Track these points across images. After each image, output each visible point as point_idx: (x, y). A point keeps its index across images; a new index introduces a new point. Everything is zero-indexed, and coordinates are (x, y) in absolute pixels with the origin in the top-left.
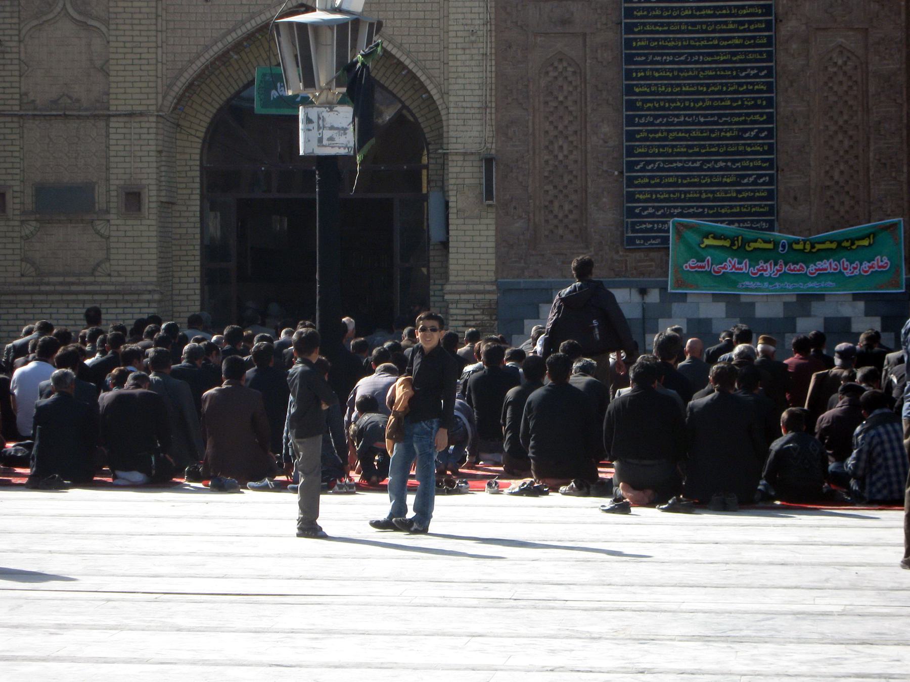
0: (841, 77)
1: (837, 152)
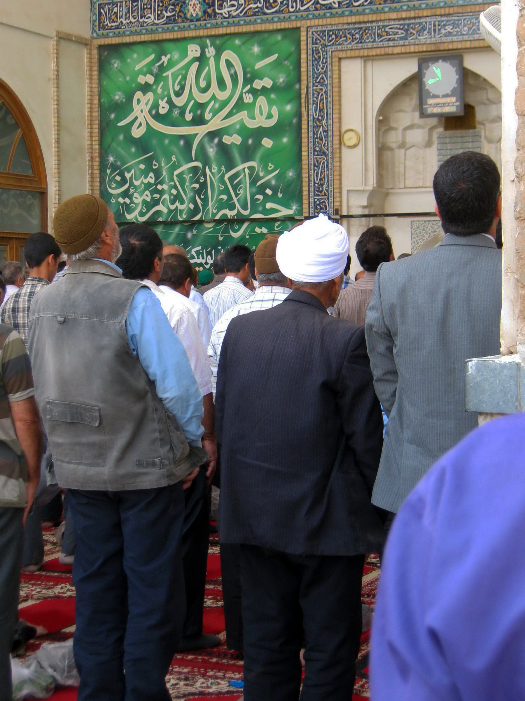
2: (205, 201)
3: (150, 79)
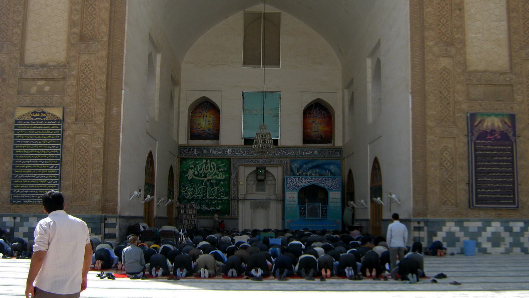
0: (84, 150)
1: (80, 174)
2: (206, 195)
3: (193, 166)
